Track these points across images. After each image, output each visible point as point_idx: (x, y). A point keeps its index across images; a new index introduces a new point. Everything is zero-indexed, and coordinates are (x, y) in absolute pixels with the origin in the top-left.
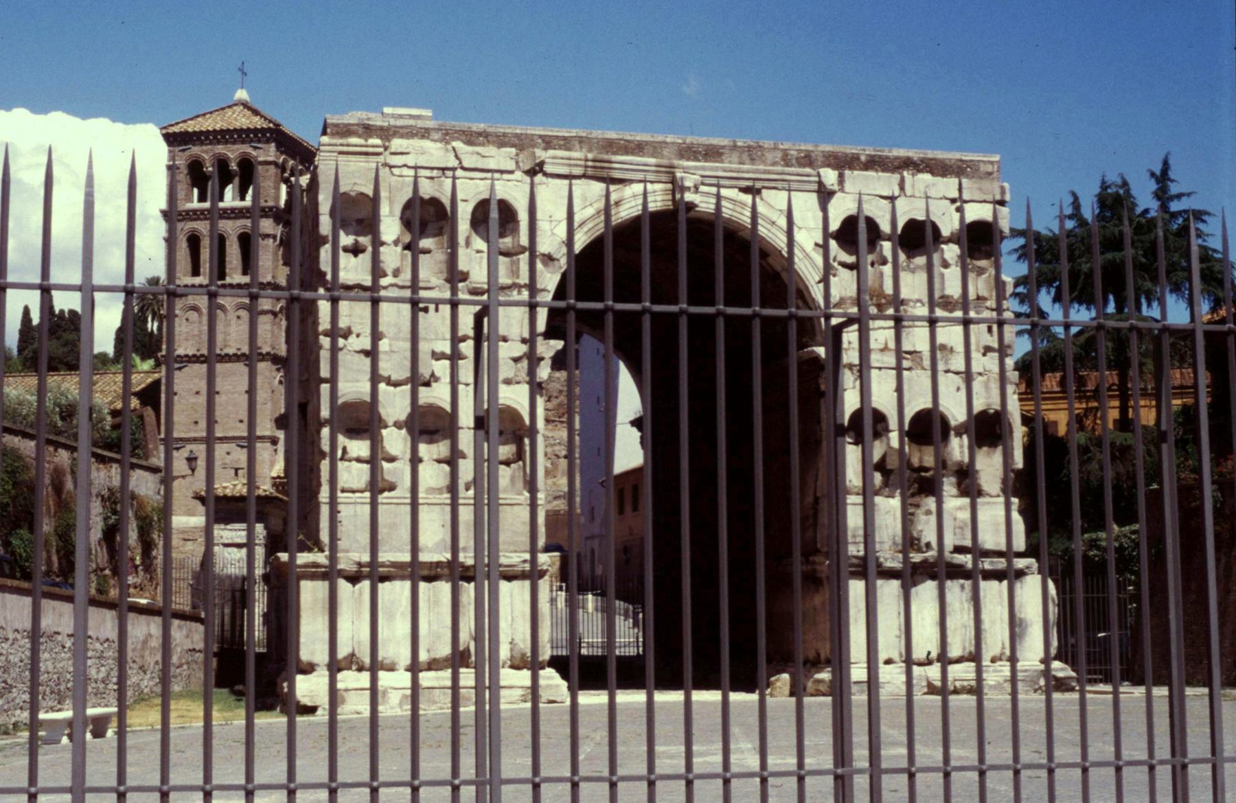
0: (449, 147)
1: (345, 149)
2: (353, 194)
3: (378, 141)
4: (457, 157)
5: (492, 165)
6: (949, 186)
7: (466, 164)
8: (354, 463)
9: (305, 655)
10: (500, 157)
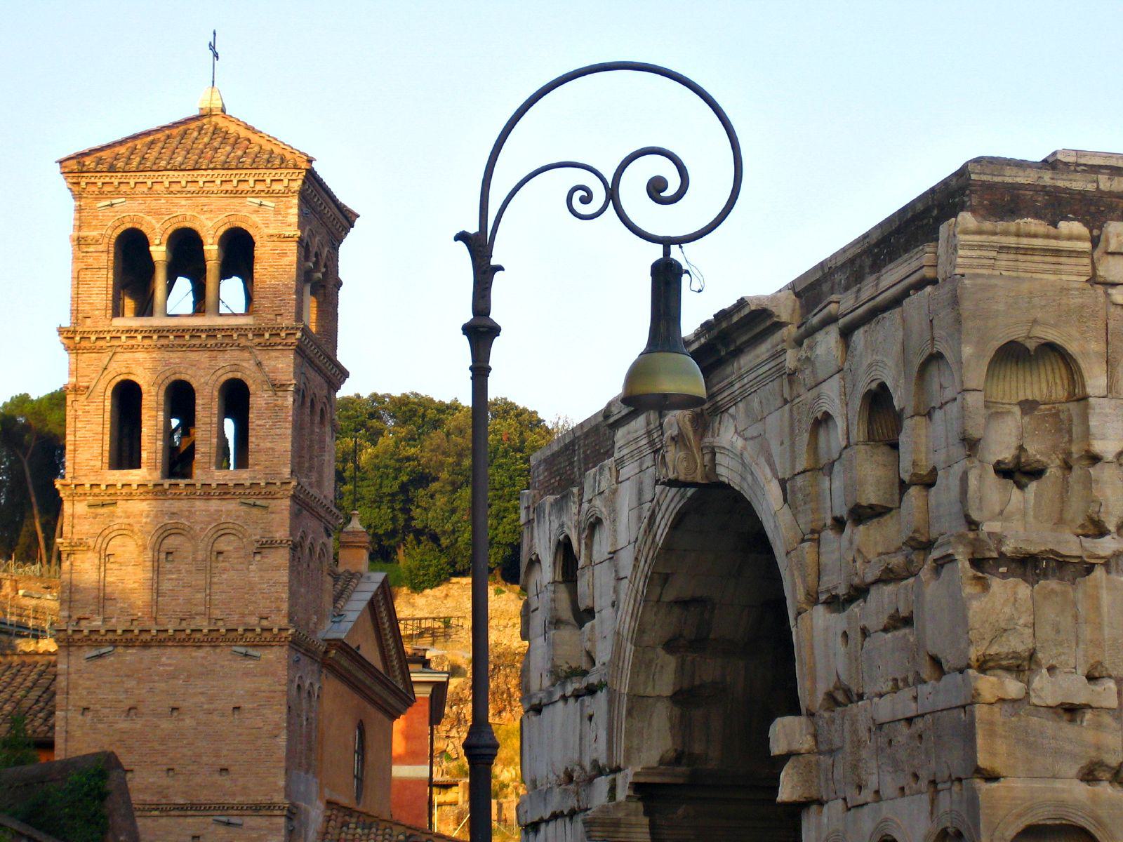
1: (1012, 241)
2: (1031, 345)
3: (1077, 227)
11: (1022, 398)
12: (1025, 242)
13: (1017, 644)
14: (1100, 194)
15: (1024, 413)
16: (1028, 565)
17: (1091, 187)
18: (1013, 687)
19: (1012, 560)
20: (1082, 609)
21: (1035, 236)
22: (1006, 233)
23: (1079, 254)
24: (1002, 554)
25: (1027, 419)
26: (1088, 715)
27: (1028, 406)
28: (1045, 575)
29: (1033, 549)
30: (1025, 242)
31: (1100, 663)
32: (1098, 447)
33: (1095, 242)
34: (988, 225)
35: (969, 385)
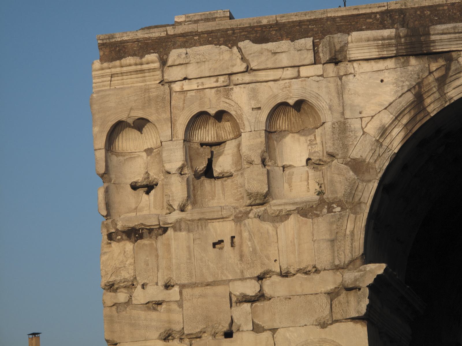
0: (235, 49)
1: (118, 70)
3: (153, 57)
4: (243, 59)
5: (284, 60)
7: (254, 65)
11: (146, 148)
12: (125, 69)
13: (126, 274)
14: (169, 37)
15: (148, 155)
16: (134, 234)
17: (163, 34)
18: (122, 297)
19: (124, 232)
20: (160, 253)
21: (130, 65)
22: (115, 67)
23: (154, 70)
24: (117, 230)
25: (149, 158)
26: (164, 306)
27: (149, 151)
28: (141, 237)
29: (131, 225)
30: (125, 69)
31: (171, 278)
33: (163, 63)
34: (105, 65)
35: (97, 147)
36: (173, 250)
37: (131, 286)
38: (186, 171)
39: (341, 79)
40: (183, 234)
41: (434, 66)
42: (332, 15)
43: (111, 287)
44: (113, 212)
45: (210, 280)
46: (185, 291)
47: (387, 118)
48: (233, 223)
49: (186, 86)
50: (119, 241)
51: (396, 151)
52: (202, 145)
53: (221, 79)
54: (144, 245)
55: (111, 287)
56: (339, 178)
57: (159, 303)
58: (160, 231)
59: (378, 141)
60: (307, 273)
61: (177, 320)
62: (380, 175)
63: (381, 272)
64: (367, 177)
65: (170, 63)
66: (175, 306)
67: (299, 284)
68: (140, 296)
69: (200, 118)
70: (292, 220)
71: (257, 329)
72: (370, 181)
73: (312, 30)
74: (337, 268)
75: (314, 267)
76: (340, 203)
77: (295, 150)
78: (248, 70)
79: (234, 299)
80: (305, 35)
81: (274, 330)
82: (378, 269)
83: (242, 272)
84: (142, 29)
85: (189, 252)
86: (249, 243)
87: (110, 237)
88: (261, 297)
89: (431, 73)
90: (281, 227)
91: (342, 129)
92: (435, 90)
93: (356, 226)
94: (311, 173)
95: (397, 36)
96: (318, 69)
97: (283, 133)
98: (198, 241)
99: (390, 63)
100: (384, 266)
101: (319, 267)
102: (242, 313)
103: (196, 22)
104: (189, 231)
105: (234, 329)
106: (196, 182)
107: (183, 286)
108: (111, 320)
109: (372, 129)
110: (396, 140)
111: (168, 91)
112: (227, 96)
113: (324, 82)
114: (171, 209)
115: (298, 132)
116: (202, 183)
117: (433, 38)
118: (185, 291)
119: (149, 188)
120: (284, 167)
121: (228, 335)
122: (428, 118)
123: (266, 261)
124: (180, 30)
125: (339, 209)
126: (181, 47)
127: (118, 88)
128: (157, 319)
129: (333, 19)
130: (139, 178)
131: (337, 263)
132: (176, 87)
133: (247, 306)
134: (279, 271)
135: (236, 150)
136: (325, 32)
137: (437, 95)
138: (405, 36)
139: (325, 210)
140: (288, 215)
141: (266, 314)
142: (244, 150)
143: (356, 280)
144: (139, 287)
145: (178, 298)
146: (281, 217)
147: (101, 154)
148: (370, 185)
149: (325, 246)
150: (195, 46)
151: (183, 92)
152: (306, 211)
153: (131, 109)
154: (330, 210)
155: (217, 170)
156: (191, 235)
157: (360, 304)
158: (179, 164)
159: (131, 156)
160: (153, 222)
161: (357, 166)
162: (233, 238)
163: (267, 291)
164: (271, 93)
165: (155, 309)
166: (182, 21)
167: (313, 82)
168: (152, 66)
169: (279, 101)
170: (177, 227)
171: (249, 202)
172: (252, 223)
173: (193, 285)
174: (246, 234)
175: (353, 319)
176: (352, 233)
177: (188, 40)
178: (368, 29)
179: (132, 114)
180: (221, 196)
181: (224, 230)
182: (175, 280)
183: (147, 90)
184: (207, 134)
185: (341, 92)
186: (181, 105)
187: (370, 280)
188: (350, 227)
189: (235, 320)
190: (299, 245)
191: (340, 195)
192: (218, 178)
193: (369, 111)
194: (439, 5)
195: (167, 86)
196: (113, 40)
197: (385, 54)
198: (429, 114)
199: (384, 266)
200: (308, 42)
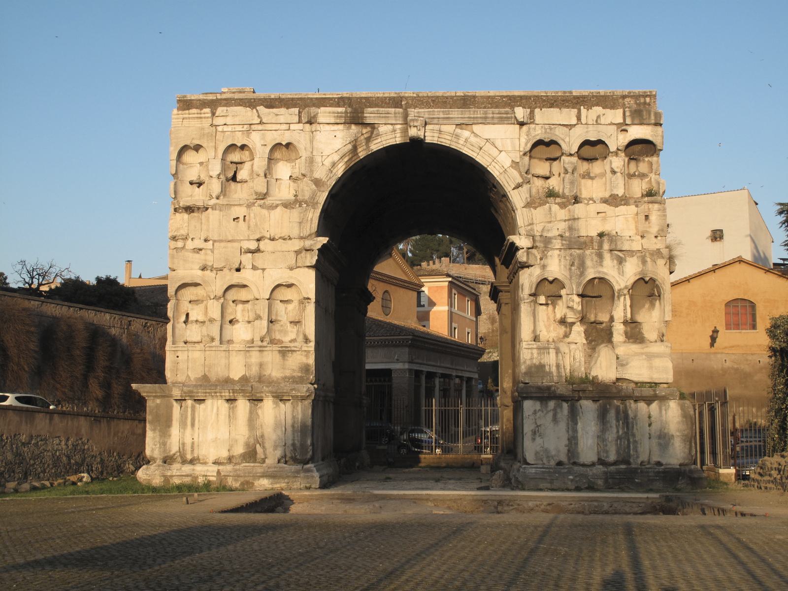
1: (187, 116)
3: (208, 110)
4: (259, 116)
5: (282, 119)
6: (616, 115)
7: (264, 121)
8: (194, 324)
9: (148, 452)
10: (289, 115)
12: (191, 116)
13: (183, 232)
14: (217, 100)
16: (189, 209)
17: (215, 98)
18: (180, 244)
19: (183, 208)
20: (203, 221)
21: (194, 114)
22: (185, 114)
26: (203, 251)
27: (201, 164)
28: (193, 211)
29: (188, 204)
30: (191, 116)
32: (211, 173)
33: (213, 114)
34: (180, 112)
36: (210, 220)
37: (185, 239)
38: (221, 176)
39: (312, 133)
40: (217, 212)
41: (364, 131)
42: (311, 96)
43: (174, 238)
44: (178, 196)
45: (230, 238)
46: (216, 244)
47: (336, 157)
48: (245, 208)
49: (226, 128)
50: (180, 213)
51: (340, 176)
52: (231, 163)
53: (246, 126)
54: (195, 216)
55: (174, 238)
56: (307, 189)
57: (201, 250)
58: (204, 209)
59: (330, 169)
60: (284, 239)
61: (210, 259)
62: (330, 189)
63: (325, 242)
64: (322, 189)
65: (217, 115)
66: (209, 252)
67: (279, 245)
68: (190, 245)
69: (232, 147)
70: (279, 208)
71: (254, 268)
72: (324, 191)
73: (299, 104)
74: (301, 238)
75: (289, 236)
76: (306, 202)
77: (283, 170)
78: (261, 123)
79: (243, 250)
80: (295, 106)
81: (264, 270)
82: (324, 240)
83: (249, 236)
84: (203, 94)
85: (220, 222)
86: (254, 221)
87: (176, 210)
88: (258, 250)
89: (362, 134)
90: (272, 212)
91: (311, 161)
92: (364, 144)
93: (314, 216)
94: (292, 184)
95: (346, 112)
96: (300, 126)
97: (277, 160)
98: (225, 217)
99: (341, 127)
100: (327, 239)
101: (291, 236)
102: (247, 259)
103: (234, 93)
104: (220, 210)
105: (241, 267)
106: (227, 183)
107: (214, 241)
108: (173, 257)
109: (328, 163)
110: (340, 170)
111: (214, 131)
112: (248, 137)
113: (303, 134)
114: (211, 197)
115: (286, 160)
116: (230, 184)
117: (365, 115)
118: (215, 244)
119: (200, 184)
120: (276, 179)
121: (238, 270)
122: (359, 159)
123: (263, 231)
124: (224, 96)
125: (305, 205)
126: (224, 106)
127: (188, 126)
128: (199, 259)
129: (311, 99)
130: (194, 178)
131: (302, 235)
132: (220, 129)
133: (250, 255)
134: (269, 237)
135: (250, 167)
136: (306, 106)
137: (365, 147)
138: (350, 113)
139: (298, 206)
140: (277, 206)
141: (259, 260)
142: (255, 168)
143: (311, 245)
144: (190, 239)
145: (212, 248)
146: (273, 207)
147: (174, 163)
148: (324, 193)
149: (296, 225)
150: (232, 106)
151: (223, 132)
152: (287, 205)
153: (193, 139)
154: (300, 206)
155: (239, 178)
156: (221, 212)
157: (312, 259)
158: (218, 173)
159: (190, 165)
160: (200, 204)
161: (317, 182)
162: (245, 216)
163: (262, 247)
164: (273, 138)
165: (198, 253)
166: (225, 91)
167: (298, 134)
168: (207, 115)
169: (277, 142)
170: (214, 208)
171: (255, 197)
172: (256, 209)
173: (221, 241)
174: (252, 215)
175: (308, 267)
176: (312, 219)
177: (228, 102)
178: (330, 106)
179: (193, 142)
180: (240, 193)
181: (240, 212)
182: (210, 237)
183: (203, 129)
184: (235, 157)
185: (312, 141)
186: (222, 139)
187: (319, 246)
188: (310, 215)
189: (242, 262)
190: (282, 223)
191: (306, 198)
192: (239, 182)
193: (326, 153)
194: (370, 97)
195: (214, 127)
196: (186, 99)
197: (338, 121)
198: (359, 157)
199: (327, 239)
200: (296, 110)
